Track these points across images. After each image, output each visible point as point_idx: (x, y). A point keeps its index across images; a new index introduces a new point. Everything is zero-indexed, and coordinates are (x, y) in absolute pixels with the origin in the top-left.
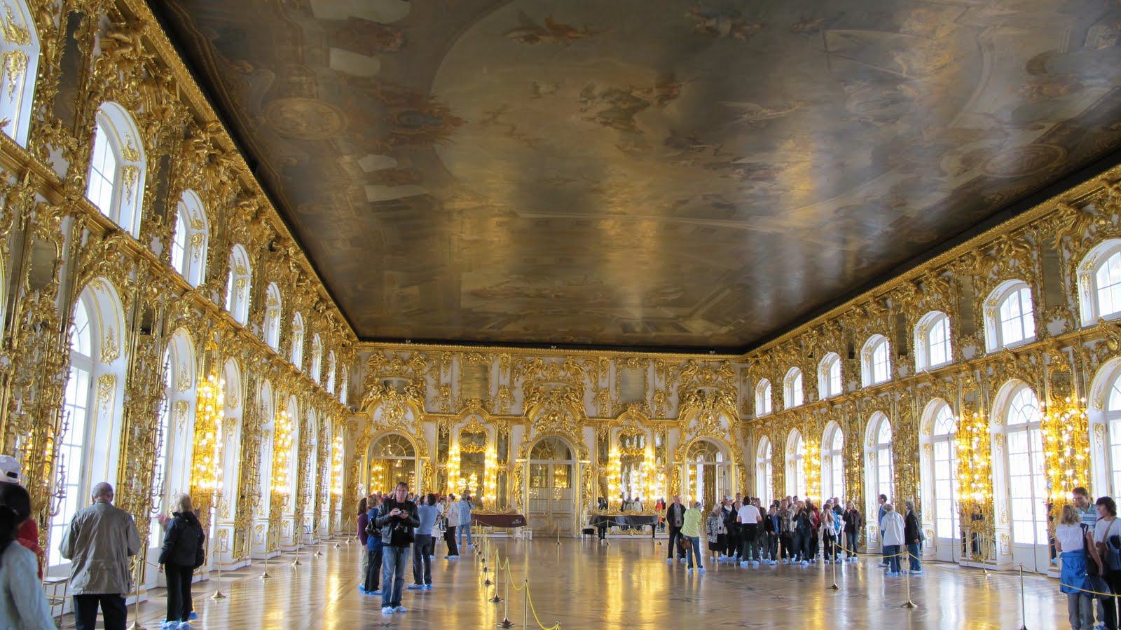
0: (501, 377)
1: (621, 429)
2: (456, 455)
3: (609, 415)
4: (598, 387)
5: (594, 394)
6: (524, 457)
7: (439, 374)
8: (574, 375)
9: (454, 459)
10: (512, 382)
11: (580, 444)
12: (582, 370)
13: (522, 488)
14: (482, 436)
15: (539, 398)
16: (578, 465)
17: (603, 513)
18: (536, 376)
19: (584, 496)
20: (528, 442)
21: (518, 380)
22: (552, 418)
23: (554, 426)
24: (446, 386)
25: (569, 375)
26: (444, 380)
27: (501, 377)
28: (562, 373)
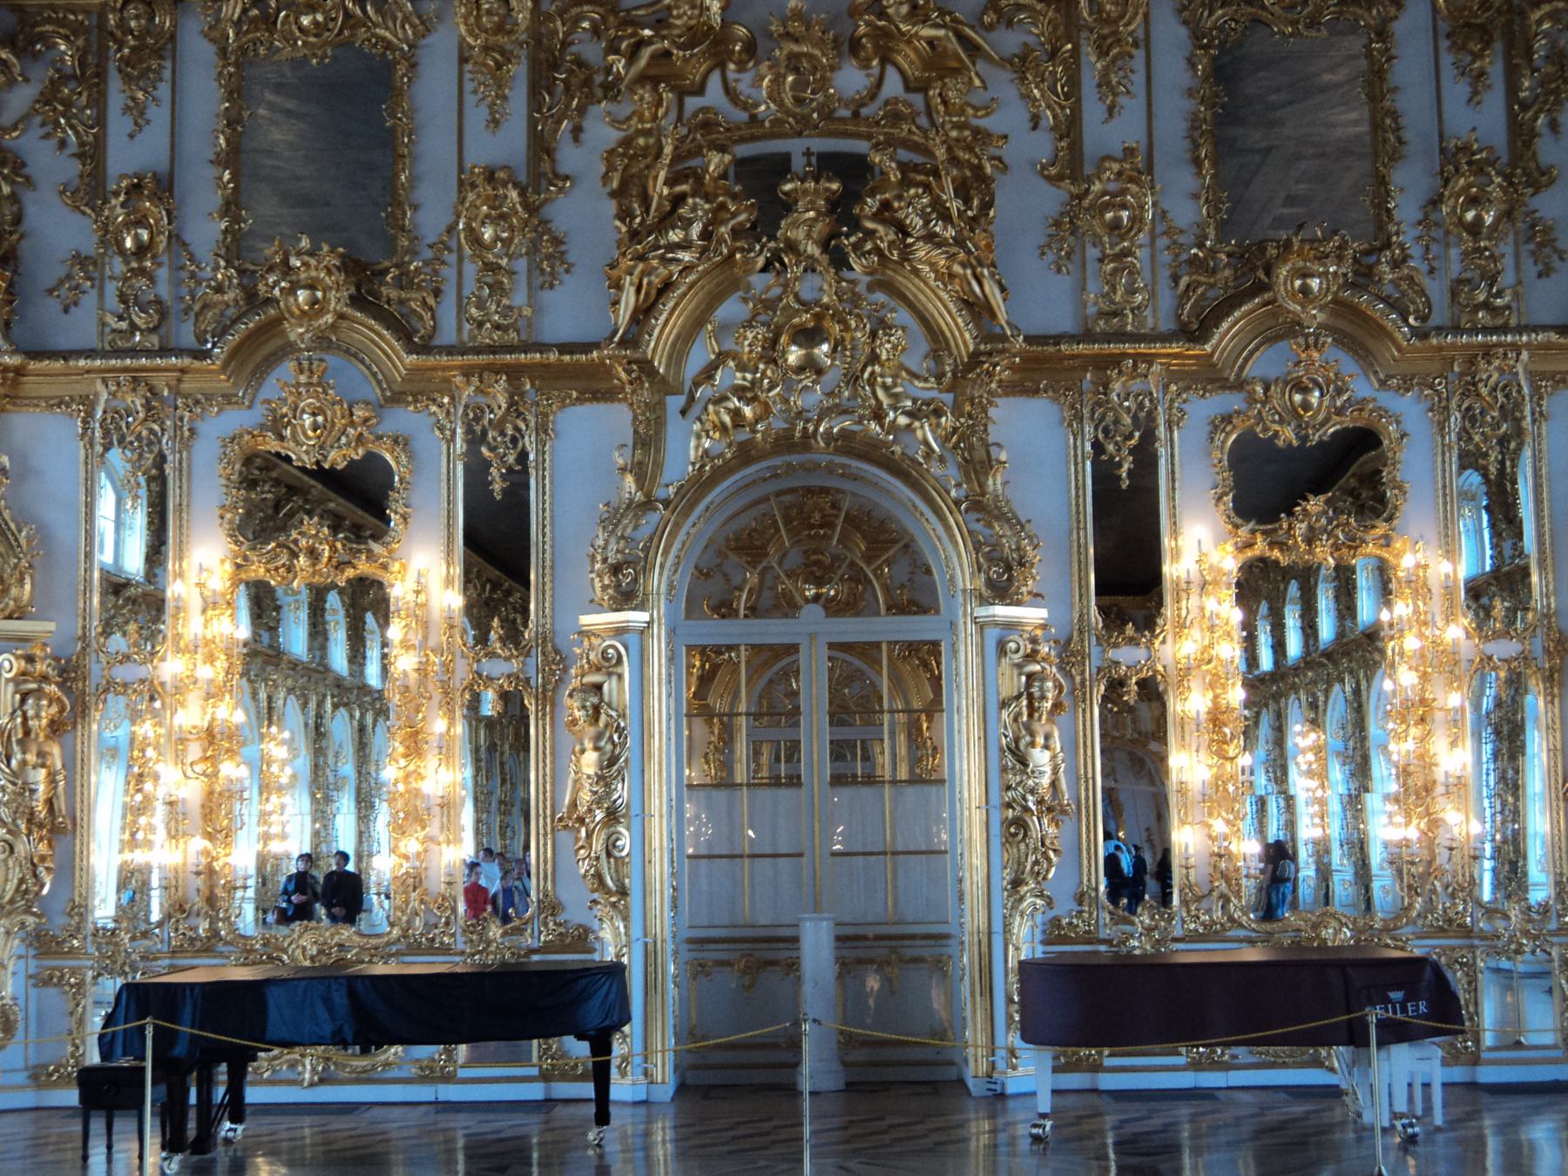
0: (477, 116)
1: (1234, 401)
2: (208, 605)
3: (1160, 316)
4: (1076, 148)
5: (1051, 199)
6: (626, 598)
7: (101, 121)
8: (921, 87)
9: (193, 626)
10: (541, 146)
11: (979, 505)
12: (972, 49)
13: (622, 792)
14: (360, 500)
15: (706, 235)
16: (967, 631)
17: (1139, 935)
18: (692, 103)
19: (1017, 827)
20: (648, 505)
21: (577, 132)
22: (794, 355)
23: (812, 397)
24: (135, 189)
25: (893, 86)
26: (129, 154)
27: (477, 116)
28: (851, 79)
